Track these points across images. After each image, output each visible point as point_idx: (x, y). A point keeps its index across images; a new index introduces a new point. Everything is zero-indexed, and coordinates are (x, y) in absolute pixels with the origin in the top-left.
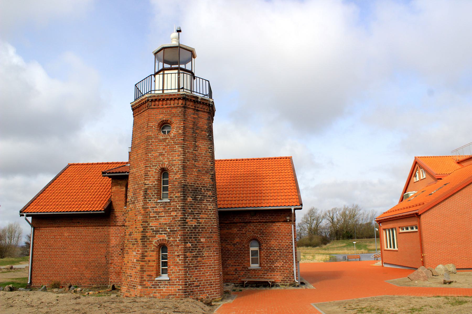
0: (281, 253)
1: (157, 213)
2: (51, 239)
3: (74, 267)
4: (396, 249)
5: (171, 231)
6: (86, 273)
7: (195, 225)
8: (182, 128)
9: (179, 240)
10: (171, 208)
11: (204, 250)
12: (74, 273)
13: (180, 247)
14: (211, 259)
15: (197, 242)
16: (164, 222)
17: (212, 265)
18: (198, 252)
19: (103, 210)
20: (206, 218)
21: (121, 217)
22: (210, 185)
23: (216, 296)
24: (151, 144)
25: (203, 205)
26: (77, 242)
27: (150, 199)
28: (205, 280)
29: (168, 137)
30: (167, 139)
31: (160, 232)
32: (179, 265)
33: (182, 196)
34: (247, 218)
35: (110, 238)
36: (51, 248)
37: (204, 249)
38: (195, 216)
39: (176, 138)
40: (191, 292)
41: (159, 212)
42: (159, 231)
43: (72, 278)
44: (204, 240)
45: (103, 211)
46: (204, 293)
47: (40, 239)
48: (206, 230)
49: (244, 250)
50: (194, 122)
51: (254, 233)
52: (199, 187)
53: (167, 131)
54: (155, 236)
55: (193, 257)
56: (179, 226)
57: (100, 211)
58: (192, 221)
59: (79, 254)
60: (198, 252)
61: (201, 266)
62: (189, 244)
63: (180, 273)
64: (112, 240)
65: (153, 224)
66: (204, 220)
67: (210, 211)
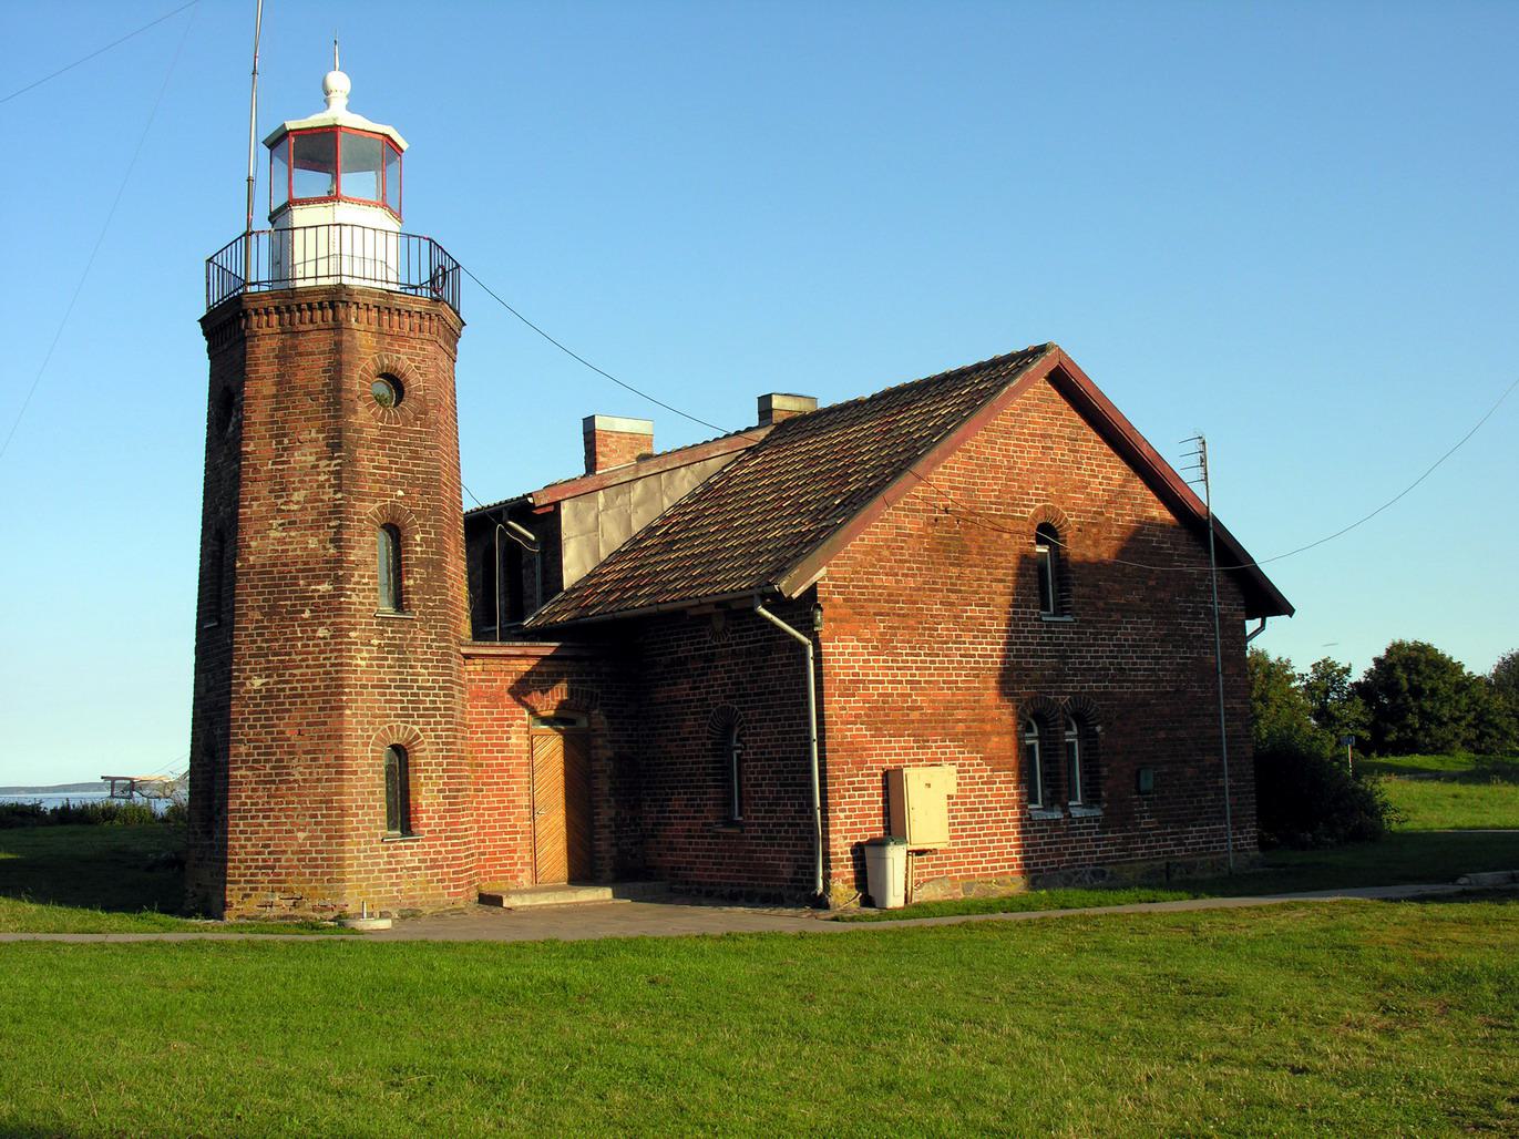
11: (295, 762)
67: (322, 642)
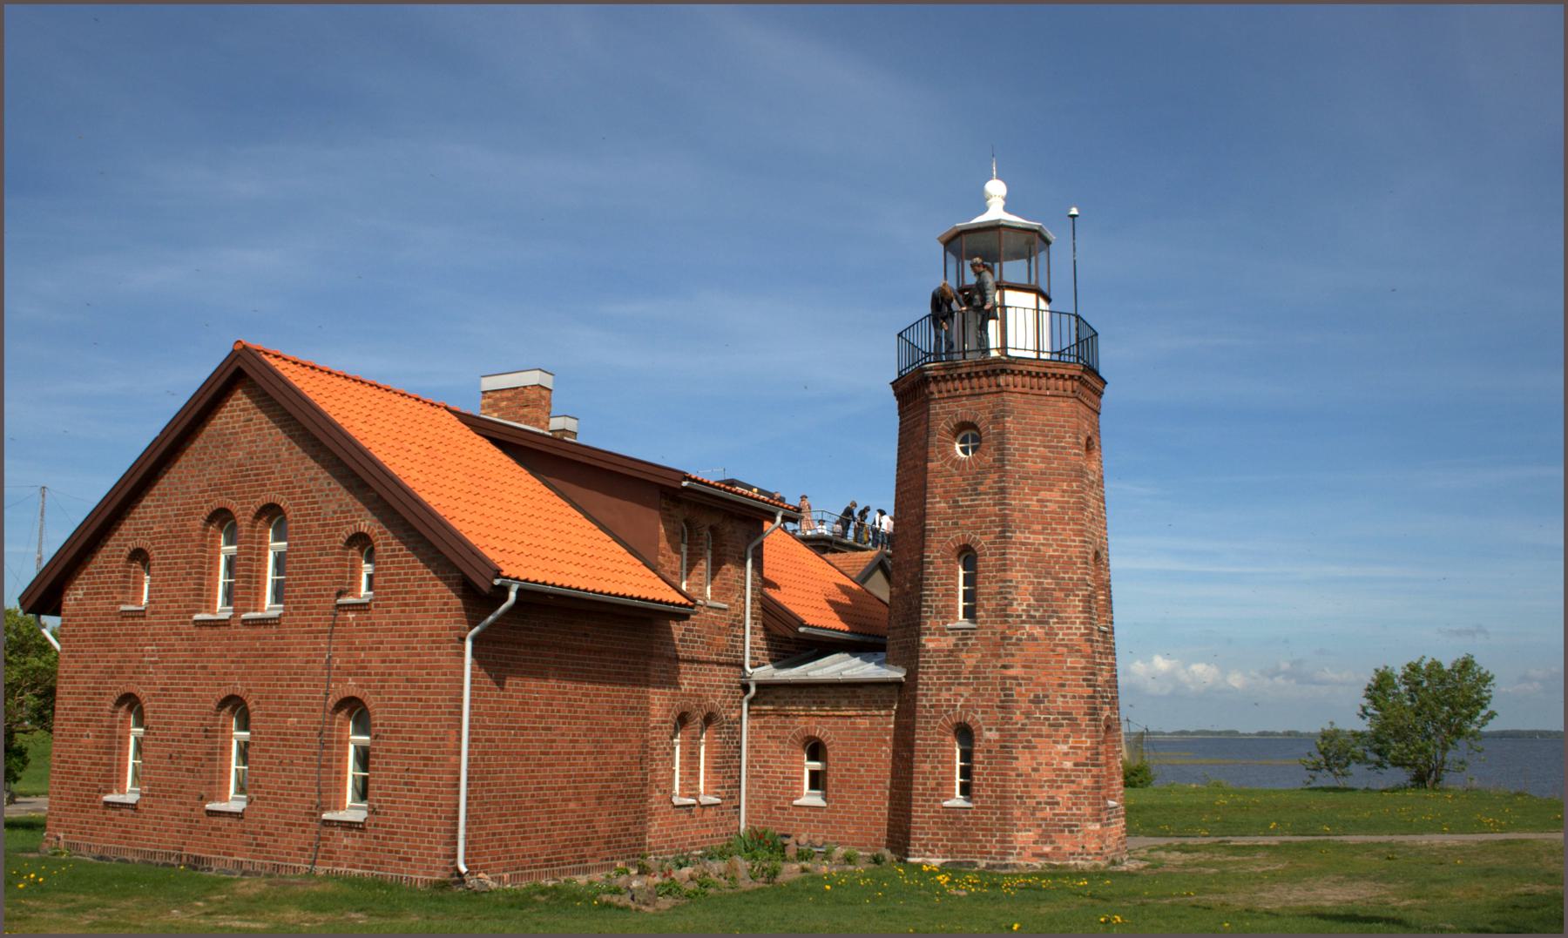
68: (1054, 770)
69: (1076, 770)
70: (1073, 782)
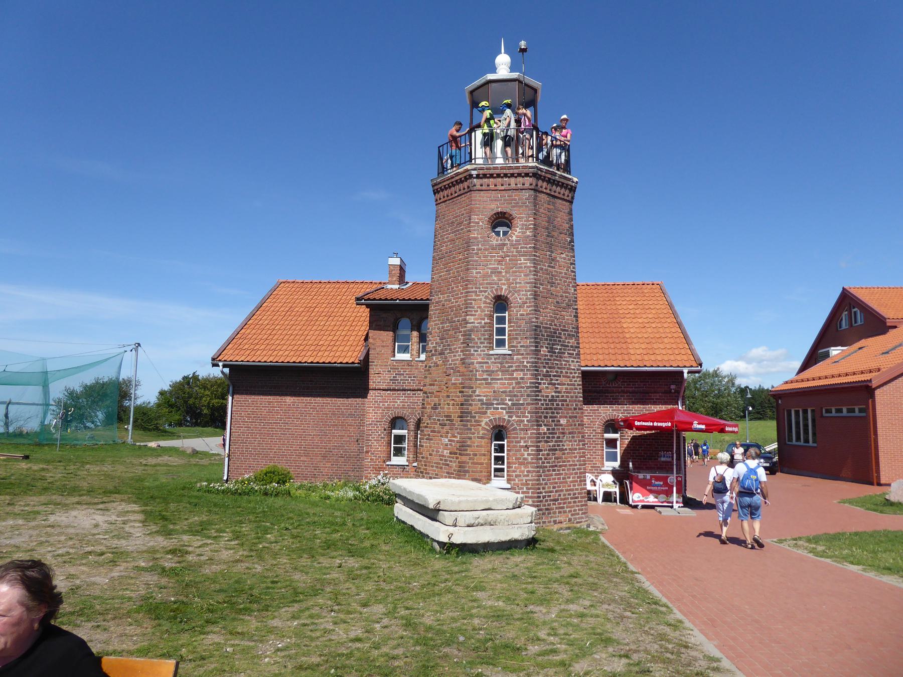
0: (659, 445)
1: (490, 372)
2: (262, 407)
3: (302, 456)
4: (811, 443)
5: (513, 404)
6: (323, 467)
7: (553, 396)
8: (532, 226)
9: (527, 421)
10: (514, 365)
12: (302, 466)
13: (529, 432)
14: (574, 453)
15: (555, 425)
16: (501, 388)
17: (576, 465)
18: (556, 442)
19: (357, 361)
20: (568, 384)
21: (386, 374)
22: (573, 328)
23: (582, 518)
24: (477, 254)
25: (564, 361)
26: (308, 414)
27: (476, 349)
28: (567, 490)
29: (507, 242)
30: (504, 245)
31: (495, 406)
32: (528, 463)
33: (532, 346)
34: (602, 384)
35: (365, 409)
36: (263, 423)
37: (565, 437)
38: (552, 380)
39: (520, 244)
40: (547, 509)
41: (493, 372)
42: (493, 404)
43: (298, 474)
44: (566, 422)
45: (358, 363)
46: (565, 512)
47: (244, 406)
48: (568, 405)
49: (595, 439)
50: (549, 218)
51: (612, 410)
52: (558, 330)
53: (501, 232)
54: (485, 413)
55: (549, 450)
56: (528, 396)
57: (353, 363)
58: (547, 388)
59: (311, 435)
60: (556, 442)
61: (560, 466)
62: (543, 427)
63: (530, 478)
64: (369, 413)
65: (481, 392)
66: (564, 387)
67: (573, 371)
68: (440, 456)
69: (450, 457)
70: (448, 465)
